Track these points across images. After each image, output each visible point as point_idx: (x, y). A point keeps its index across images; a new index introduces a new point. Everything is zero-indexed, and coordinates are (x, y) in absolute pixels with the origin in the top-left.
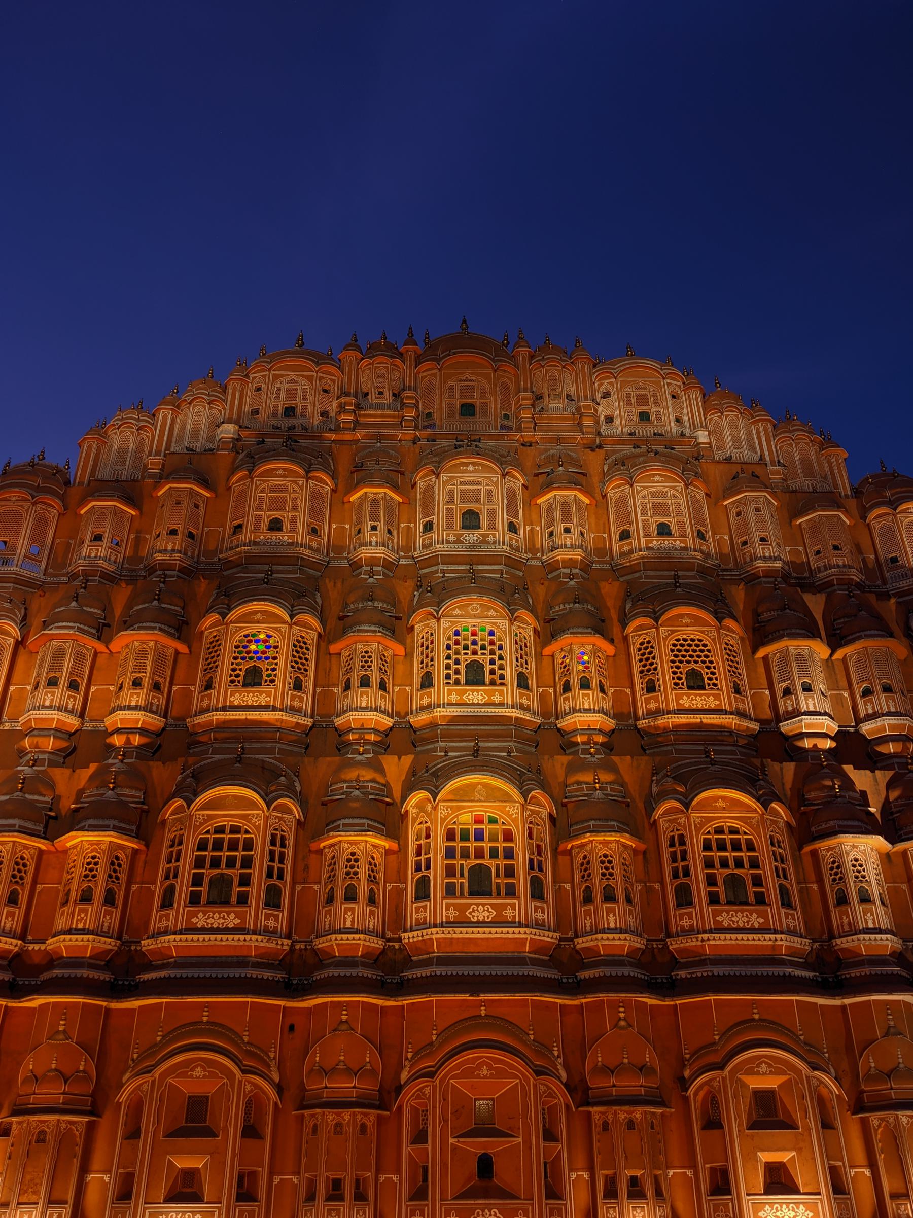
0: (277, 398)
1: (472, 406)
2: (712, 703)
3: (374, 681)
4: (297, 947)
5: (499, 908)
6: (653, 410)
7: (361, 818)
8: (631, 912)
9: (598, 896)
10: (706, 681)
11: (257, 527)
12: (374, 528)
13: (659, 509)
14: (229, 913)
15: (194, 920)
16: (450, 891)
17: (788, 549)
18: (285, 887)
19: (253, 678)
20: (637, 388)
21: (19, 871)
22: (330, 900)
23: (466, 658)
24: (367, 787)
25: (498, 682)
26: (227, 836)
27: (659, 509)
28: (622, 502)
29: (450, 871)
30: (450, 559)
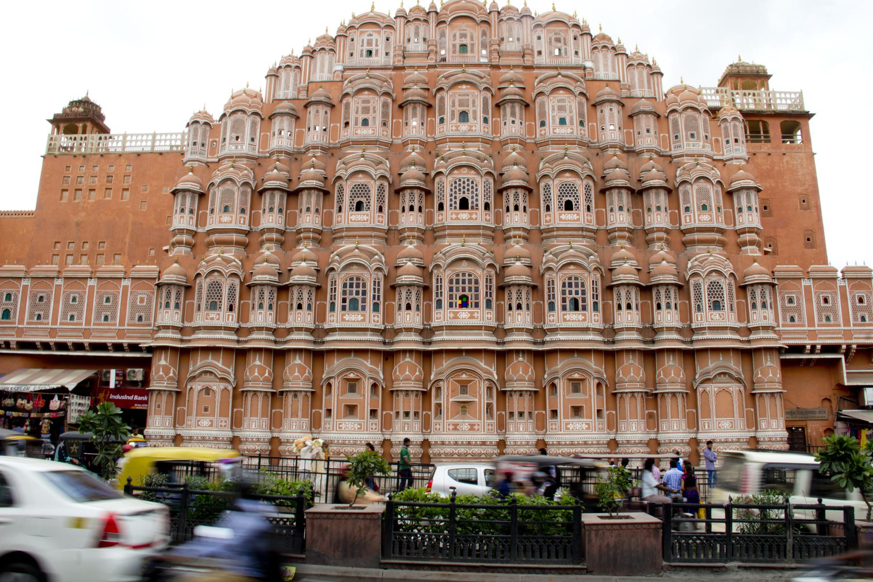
0: (362, 46)
1: (465, 45)
2: (575, 217)
3: (416, 208)
11: (356, 124)
13: (561, 108)
16: (451, 305)
19: (359, 207)
20: (556, 34)
22: (400, 309)
23: (460, 196)
26: (355, 281)
28: (542, 105)
29: (451, 297)
30: (453, 140)
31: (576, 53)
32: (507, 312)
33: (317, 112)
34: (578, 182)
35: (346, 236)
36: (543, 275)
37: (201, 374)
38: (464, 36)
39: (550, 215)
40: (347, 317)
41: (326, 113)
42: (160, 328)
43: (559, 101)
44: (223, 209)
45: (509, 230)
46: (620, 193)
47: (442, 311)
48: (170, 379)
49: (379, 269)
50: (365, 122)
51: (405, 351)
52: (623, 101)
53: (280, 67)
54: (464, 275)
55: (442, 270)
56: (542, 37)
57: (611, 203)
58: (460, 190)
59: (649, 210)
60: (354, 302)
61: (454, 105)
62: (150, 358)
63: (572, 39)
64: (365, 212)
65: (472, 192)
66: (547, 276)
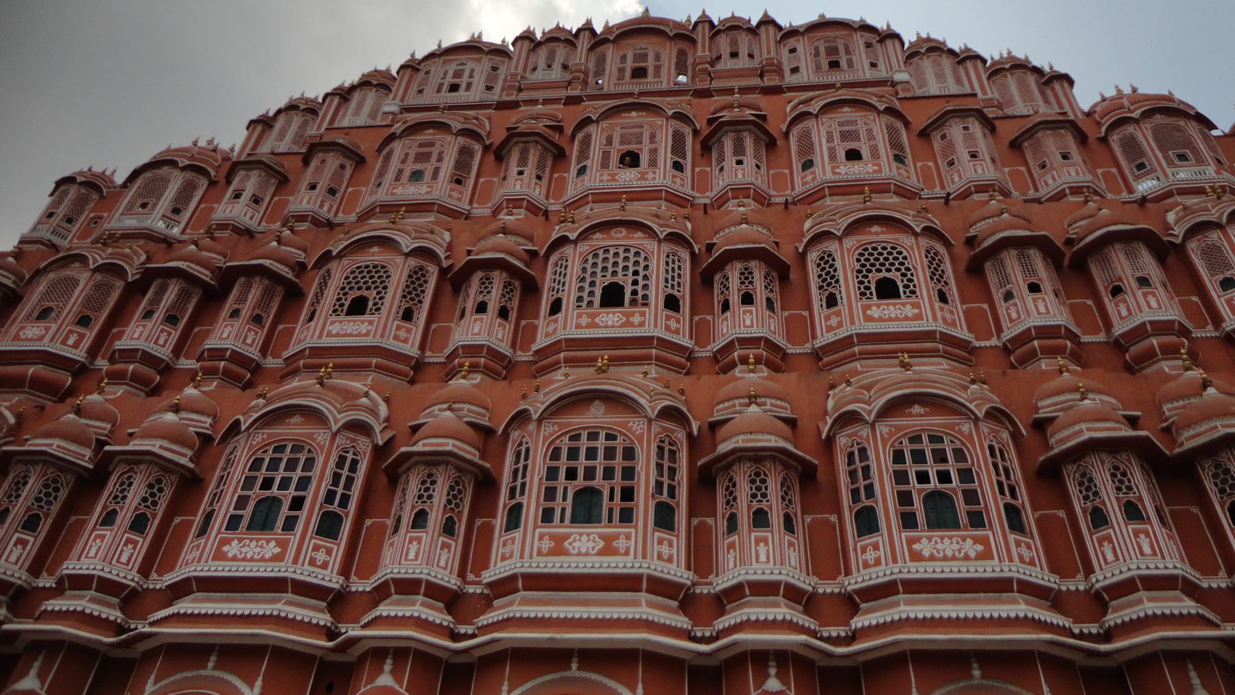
2: (909, 311)
4: (353, 589)
5: (609, 540)
7: (446, 437)
8: (791, 544)
9: (744, 519)
10: (901, 289)
12: (521, 173)
14: (268, 541)
15: (225, 548)
16: (547, 516)
17: (1006, 170)
18: (347, 517)
19: (358, 307)
21: (48, 495)
24: (462, 409)
25: (640, 301)
26: (286, 456)
29: (550, 494)
31: (873, 65)
32: (723, 542)
33: (323, 162)
34: (906, 240)
35: (305, 366)
36: (830, 440)
39: (838, 314)
40: (232, 549)
41: (342, 167)
43: (840, 124)
45: (729, 347)
46: (1022, 257)
47: (517, 535)
49: (358, 427)
50: (417, 176)
51: (378, 654)
52: (997, 123)
53: (279, 112)
54: (593, 436)
55: (532, 427)
56: (800, 48)
57: (1005, 280)
58: (605, 269)
60: (268, 507)
61: (609, 141)
63: (862, 47)
64: (366, 317)
65: (636, 273)
66: (842, 441)
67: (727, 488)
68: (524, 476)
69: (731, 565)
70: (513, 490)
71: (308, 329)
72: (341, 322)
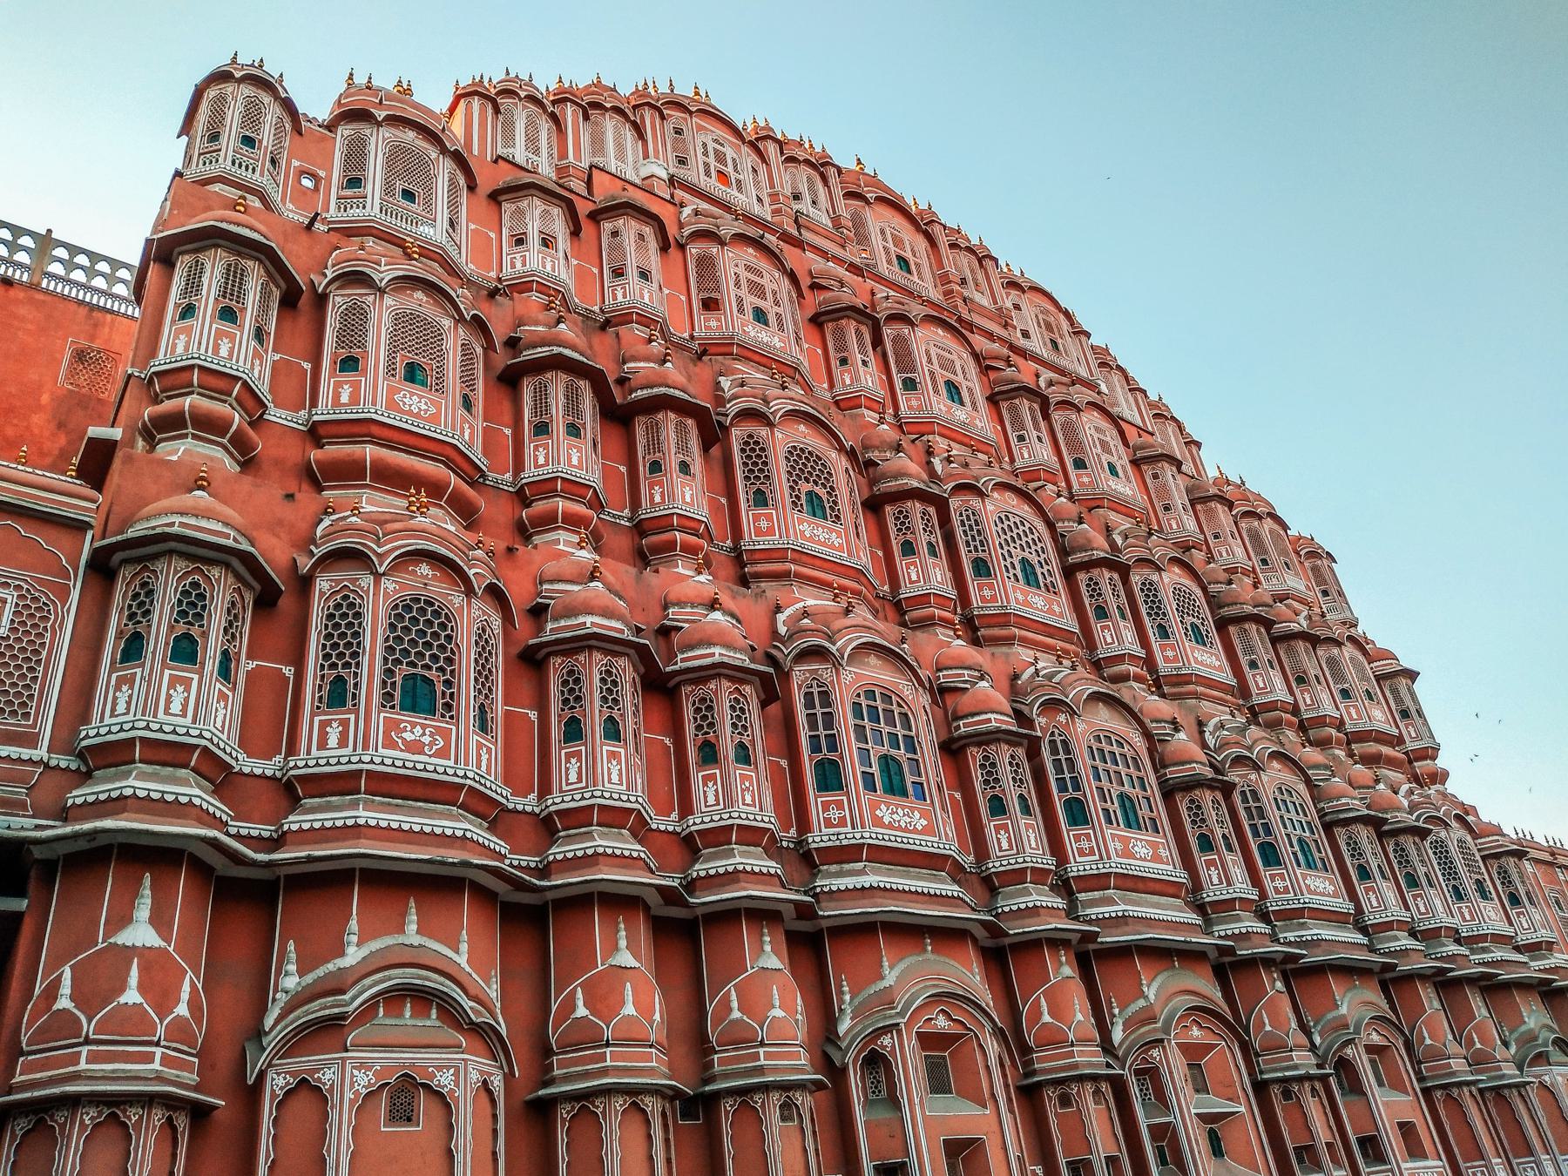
5: (1154, 845)
6: (1059, 341)
12: (864, 363)
14: (912, 809)
23: (1018, 554)
27: (1105, 446)
32: (1201, 859)
35: (797, 575)
37: (369, 1010)
38: (898, 242)
40: (884, 813)
42: (115, 755)
43: (1097, 429)
44: (401, 370)
45: (1119, 659)
48: (180, 1031)
50: (760, 316)
55: (1062, 718)
57: (1249, 650)
59: (1301, 680)
61: (930, 361)
62: (18, 917)
67: (1189, 809)
68: (1072, 767)
69: (1216, 881)
70: (1062, 784)
71: (769, 517)
72: (809, 523)
